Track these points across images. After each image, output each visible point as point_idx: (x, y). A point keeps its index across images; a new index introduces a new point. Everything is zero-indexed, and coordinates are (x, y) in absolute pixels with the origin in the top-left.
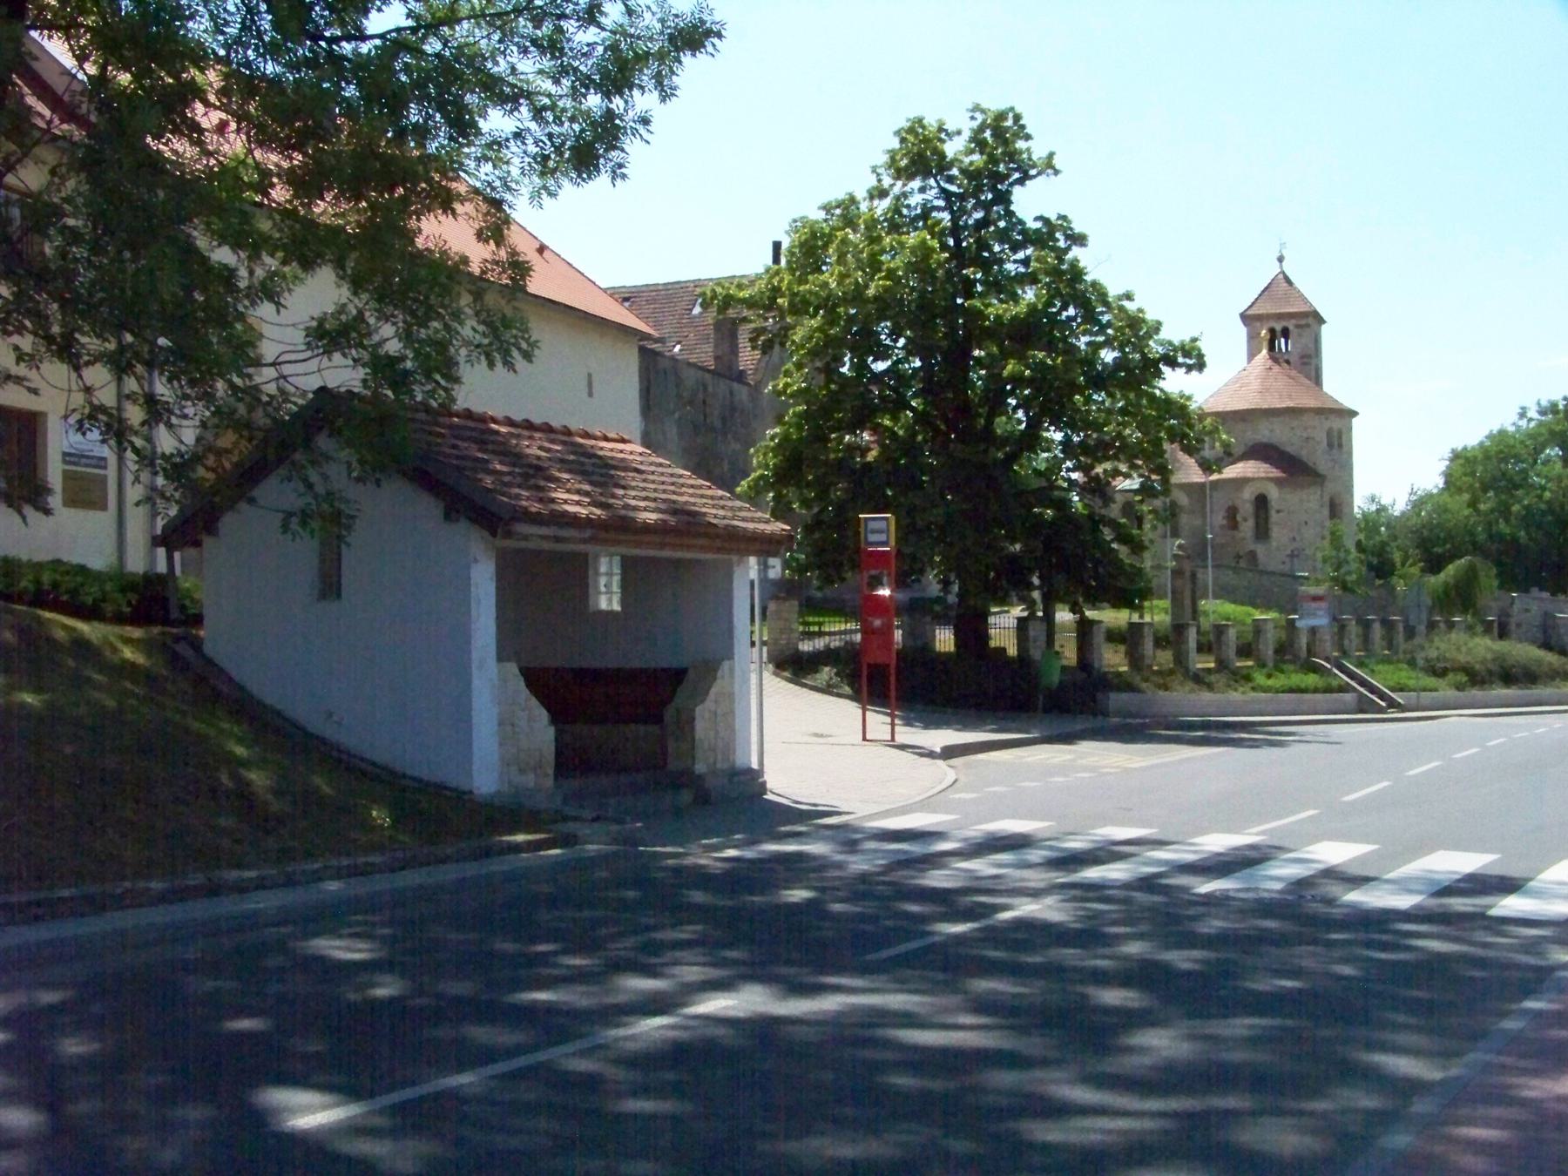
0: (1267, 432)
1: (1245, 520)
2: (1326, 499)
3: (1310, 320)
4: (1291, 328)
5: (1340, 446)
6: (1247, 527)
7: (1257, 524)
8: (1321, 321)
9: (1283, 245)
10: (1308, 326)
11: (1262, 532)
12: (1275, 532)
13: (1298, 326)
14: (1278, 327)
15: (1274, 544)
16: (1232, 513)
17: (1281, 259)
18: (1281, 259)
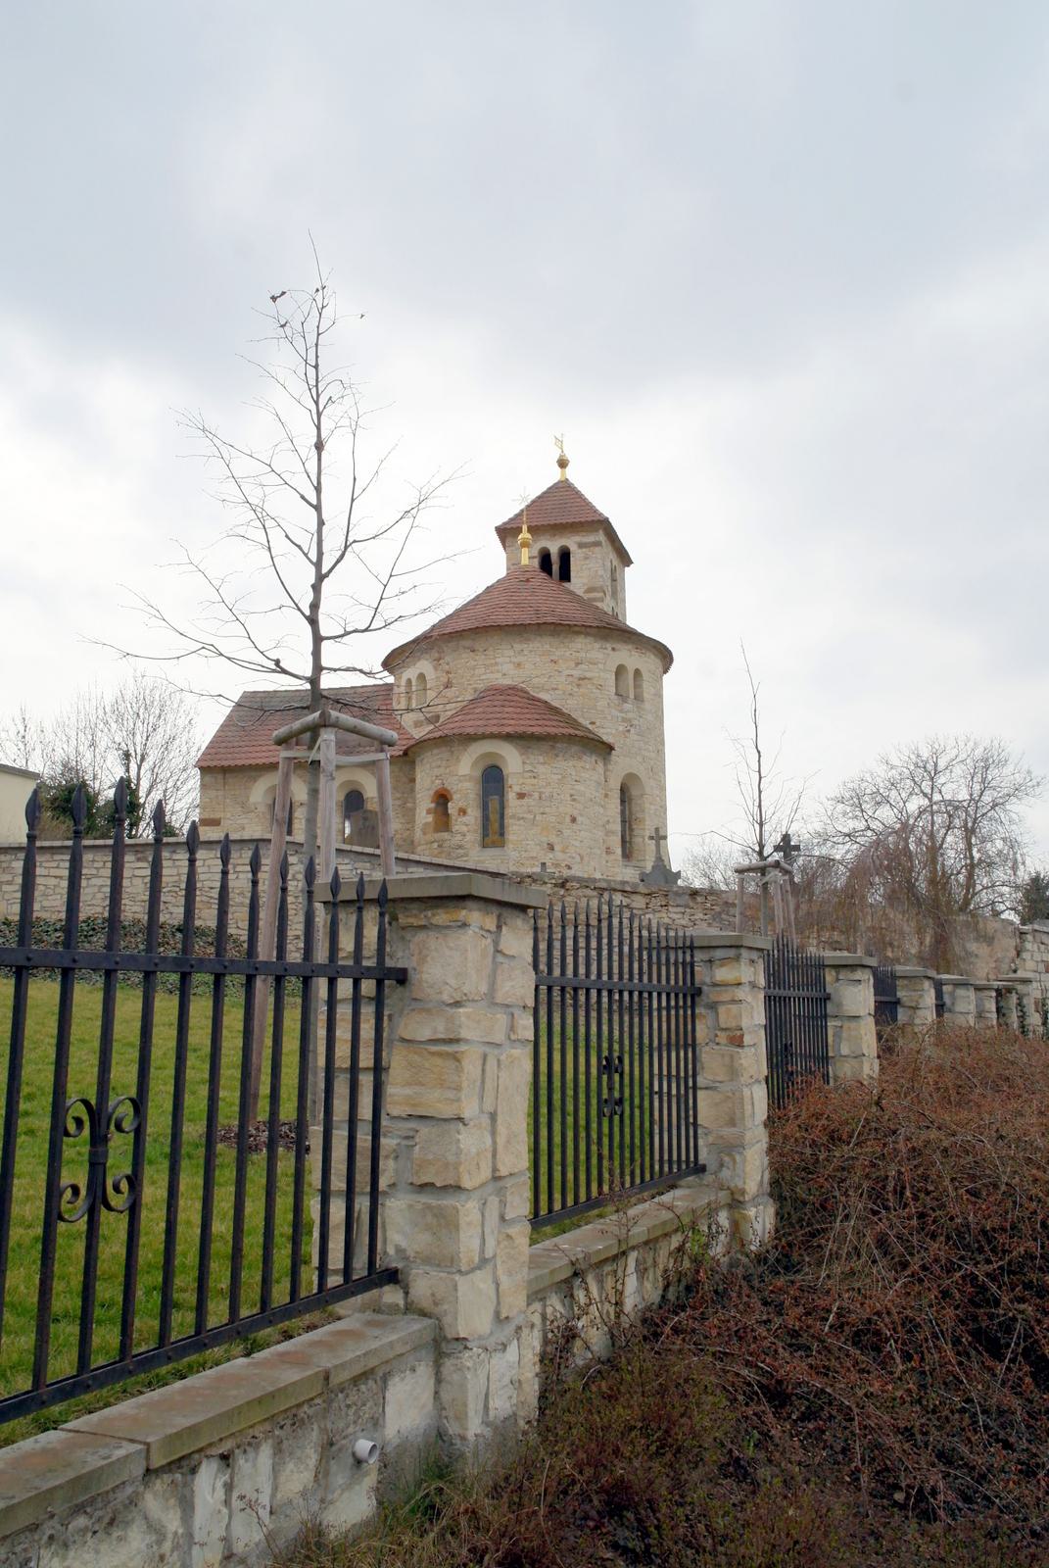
0: (508, 668)
1: (463, 812)
2: (615, 784)
3: (601, 537)
4: (573, 548)
5: (639, 698)
6: (467, 824)
7: (485, 818)
8: (625, 559)
9: (559, 442)
10: (598, 544)
11: (493, 831)
12: (514, 831)
13: (581, 546)
14: (554, 547)
15: (514, 855)
16: (442, 799)
17: (563, 463)
18: (563, 463)
